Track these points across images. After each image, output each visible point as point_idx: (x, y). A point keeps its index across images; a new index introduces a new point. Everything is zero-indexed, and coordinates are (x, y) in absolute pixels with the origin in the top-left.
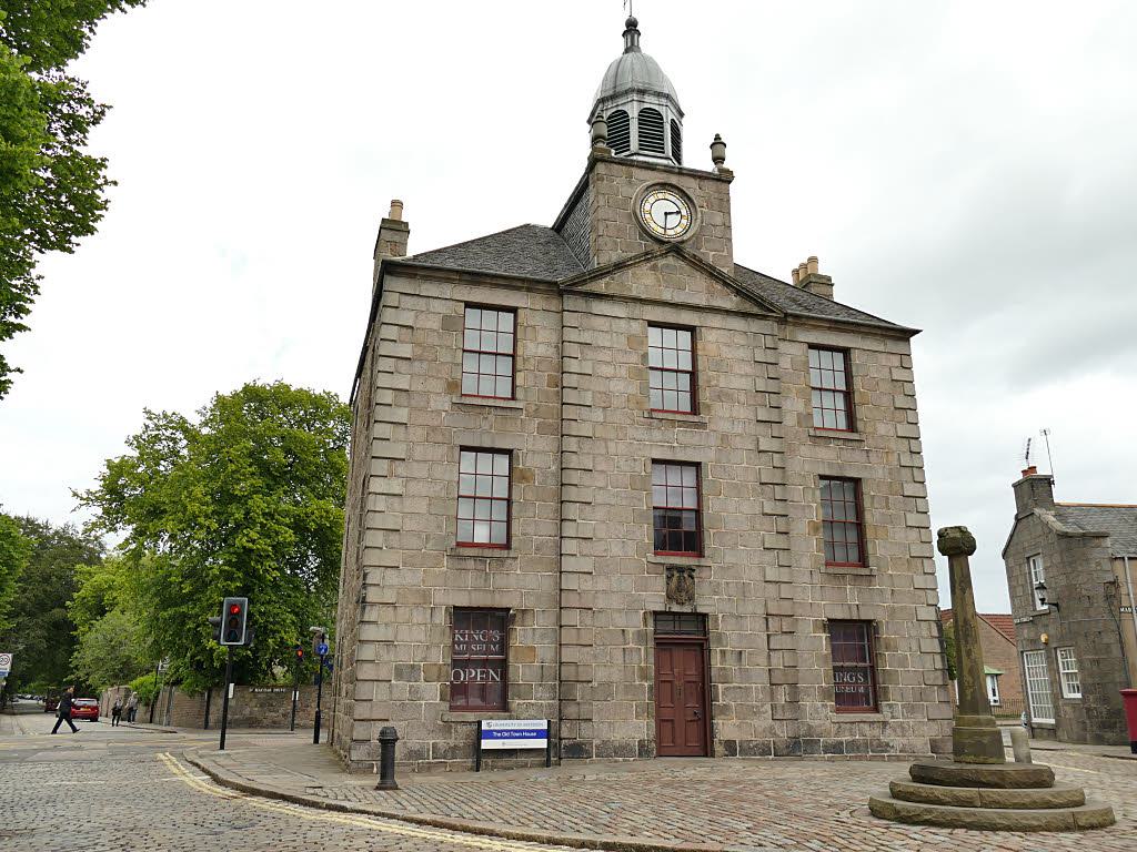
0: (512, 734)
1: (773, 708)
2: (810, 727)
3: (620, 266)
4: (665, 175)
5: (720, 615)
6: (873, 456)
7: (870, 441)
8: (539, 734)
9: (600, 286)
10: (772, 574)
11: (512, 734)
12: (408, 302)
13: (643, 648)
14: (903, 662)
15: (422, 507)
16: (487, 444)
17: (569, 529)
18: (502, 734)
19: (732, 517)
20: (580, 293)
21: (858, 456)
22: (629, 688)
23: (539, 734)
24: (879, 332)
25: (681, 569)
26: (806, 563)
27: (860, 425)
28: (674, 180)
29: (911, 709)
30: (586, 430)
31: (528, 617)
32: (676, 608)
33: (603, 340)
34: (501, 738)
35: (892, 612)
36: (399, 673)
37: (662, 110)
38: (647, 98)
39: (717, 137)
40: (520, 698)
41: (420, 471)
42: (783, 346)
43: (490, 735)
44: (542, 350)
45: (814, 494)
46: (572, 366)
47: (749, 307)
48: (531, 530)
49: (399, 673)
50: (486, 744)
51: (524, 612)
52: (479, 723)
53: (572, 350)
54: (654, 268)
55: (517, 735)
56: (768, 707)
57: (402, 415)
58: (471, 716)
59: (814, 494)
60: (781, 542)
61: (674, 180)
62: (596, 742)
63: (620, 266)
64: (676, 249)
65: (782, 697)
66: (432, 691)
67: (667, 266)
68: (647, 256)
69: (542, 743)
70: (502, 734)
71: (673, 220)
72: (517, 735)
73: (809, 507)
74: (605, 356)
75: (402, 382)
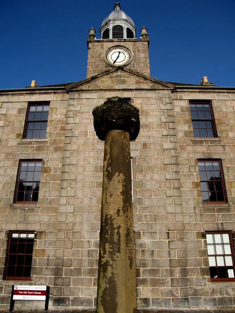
0: (28, 293)
1: (172, 280)
2: (196, 290)
4: (118, 43)
5: (142, 232)
6: (227, 148)
7: (225, 141)
8: (43, 293)
9: (84, 87)
10: (170, 209)
11: (28, 293)
13: (98, 249)
16: (31, 157)
17: (64, 193)
18: (23, 292)
20: (78, 91)
21: (220, 149)
24: (226, 91)
26: (192, 203)
27: (219, 134)
30: (74, 147)
31: (43, 235)
34: (23, 294)
37: (123, 25)
38: (116, 22)
40: (36, 274)
42: (176, 103)
43: (17, 292)
44: (59, 117)
45: (195, 169)
46: (71, 121)
47: (157, 86)
48: (47, 194)
51: (41, 233)
52: (13, 286)
53: (71, 114)
54: (111, 77)
55: (31, 293)
56: (169, 279)
58: (11, 283)
59: (195, 169)
60: (175, 192)
62: (71, 297)
64: (121, 68)
65: (177, 275)
67: (117, 76)
68: (107, 73)
70: (23, 292)
71: (114, 57)
72: (31, 293)
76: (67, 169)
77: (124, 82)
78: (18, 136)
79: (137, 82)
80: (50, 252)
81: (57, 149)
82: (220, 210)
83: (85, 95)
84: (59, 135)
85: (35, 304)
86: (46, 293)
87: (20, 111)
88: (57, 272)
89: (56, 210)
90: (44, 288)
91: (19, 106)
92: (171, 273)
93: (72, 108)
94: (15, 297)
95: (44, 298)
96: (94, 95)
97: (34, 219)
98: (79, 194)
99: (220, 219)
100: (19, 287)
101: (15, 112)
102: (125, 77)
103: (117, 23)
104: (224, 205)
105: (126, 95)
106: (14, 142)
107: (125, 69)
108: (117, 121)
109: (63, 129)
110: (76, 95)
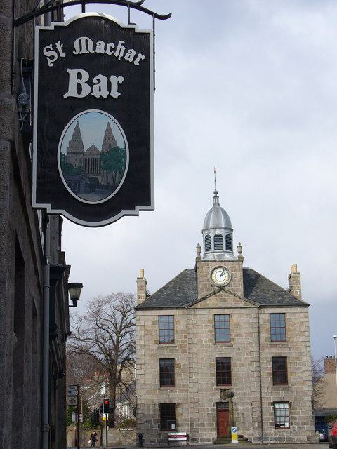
3: (204, 299)
8: (185, 436)
12: (142, 318)
14: (299, 413)
15: (150, 377)
19: (239, 372)
22: (210, 424)
23: (185, 436)
25: (225, 390)
28: (223, 264)
29: (300, 428)
32: (223, 401)
33: (199, 323)
35: (296, 398)
36: (147, 421)
39: (240, 244)
41: (149, 367)
43: (171, 437)
49: (147, 421)
50: (170, 439)
54: (216, 296)
57: (143, 351)
58: (166, 432)
61: (223, 264)
63: (204, 299)
64: (222, 288)
65: (256, 426)
66: (156, 426)
68: (213, 294)
69: (185, 439)
73: (268, 368)
74: (200, 327)
75: (142, 342)
76: (192, 365)
77: (224, 300)
78: (156, 342)
79: (235, 301)
80: (185, 414)
81: (184, 351)
82: (284, 389)
83: (198, 312)
84: (183, 341)
85: (181, 443)
86: (187, 436)
87: (154, 322)
88: (192, 426)
89: (187, 391)
90: (185, 434)
91: (152, 319)
92: (253, 424)
93: (191, 322)
94: (170, 439)
95: (185, 439)
96: (205, 312)
97: (174, 396)
98: (200, 381)
99: (282, 394)
100: (171, 434)
101: (150, 323)
102: (225, 296)
103: (218, 231)
104: (286, 386)
105: (227, 311)
106: (154, 346)
107: (226, 288)
108: (222, 332)
109: (186, 337)
110: (192, 312)
